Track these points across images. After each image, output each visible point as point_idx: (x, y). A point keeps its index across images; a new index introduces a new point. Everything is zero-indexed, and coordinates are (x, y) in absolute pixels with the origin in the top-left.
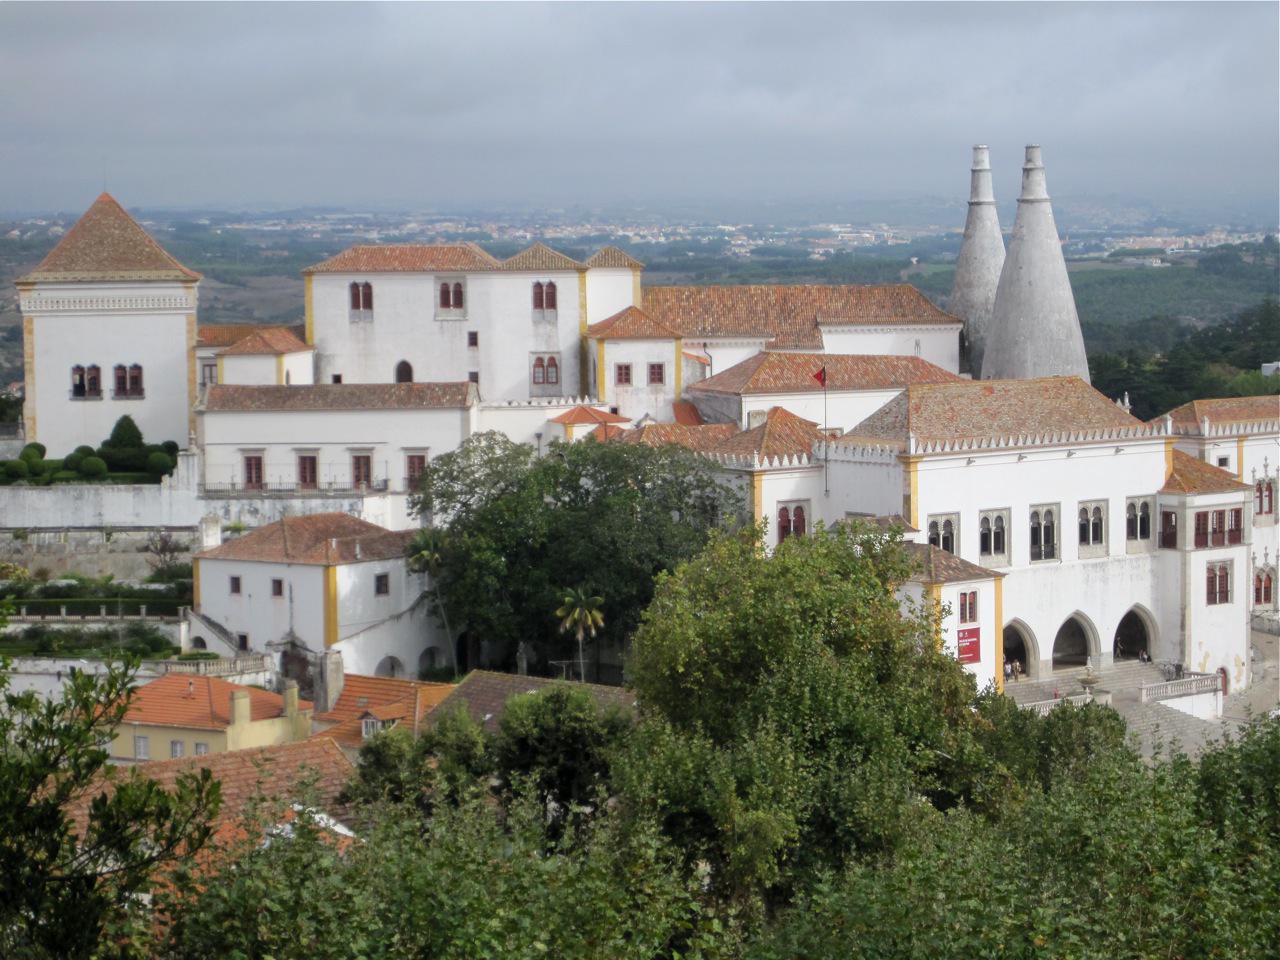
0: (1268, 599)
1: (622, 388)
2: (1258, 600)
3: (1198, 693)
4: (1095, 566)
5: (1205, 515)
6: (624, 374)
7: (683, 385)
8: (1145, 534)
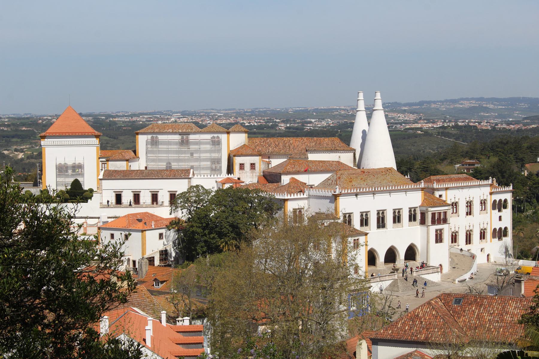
0: (455, 242)
1: (241, 171)
2: (452, 242)
5: (435, 213)
6: (242, 166)
7: (262, 170)
8: (415, 220)
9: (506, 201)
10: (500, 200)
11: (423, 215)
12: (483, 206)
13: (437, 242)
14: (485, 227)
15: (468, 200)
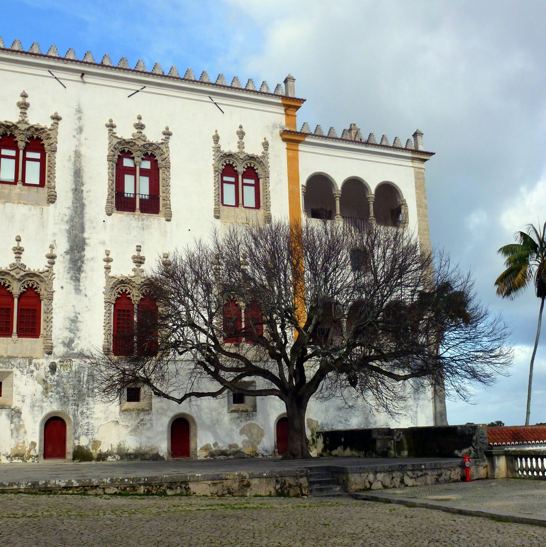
15: (126, 132)
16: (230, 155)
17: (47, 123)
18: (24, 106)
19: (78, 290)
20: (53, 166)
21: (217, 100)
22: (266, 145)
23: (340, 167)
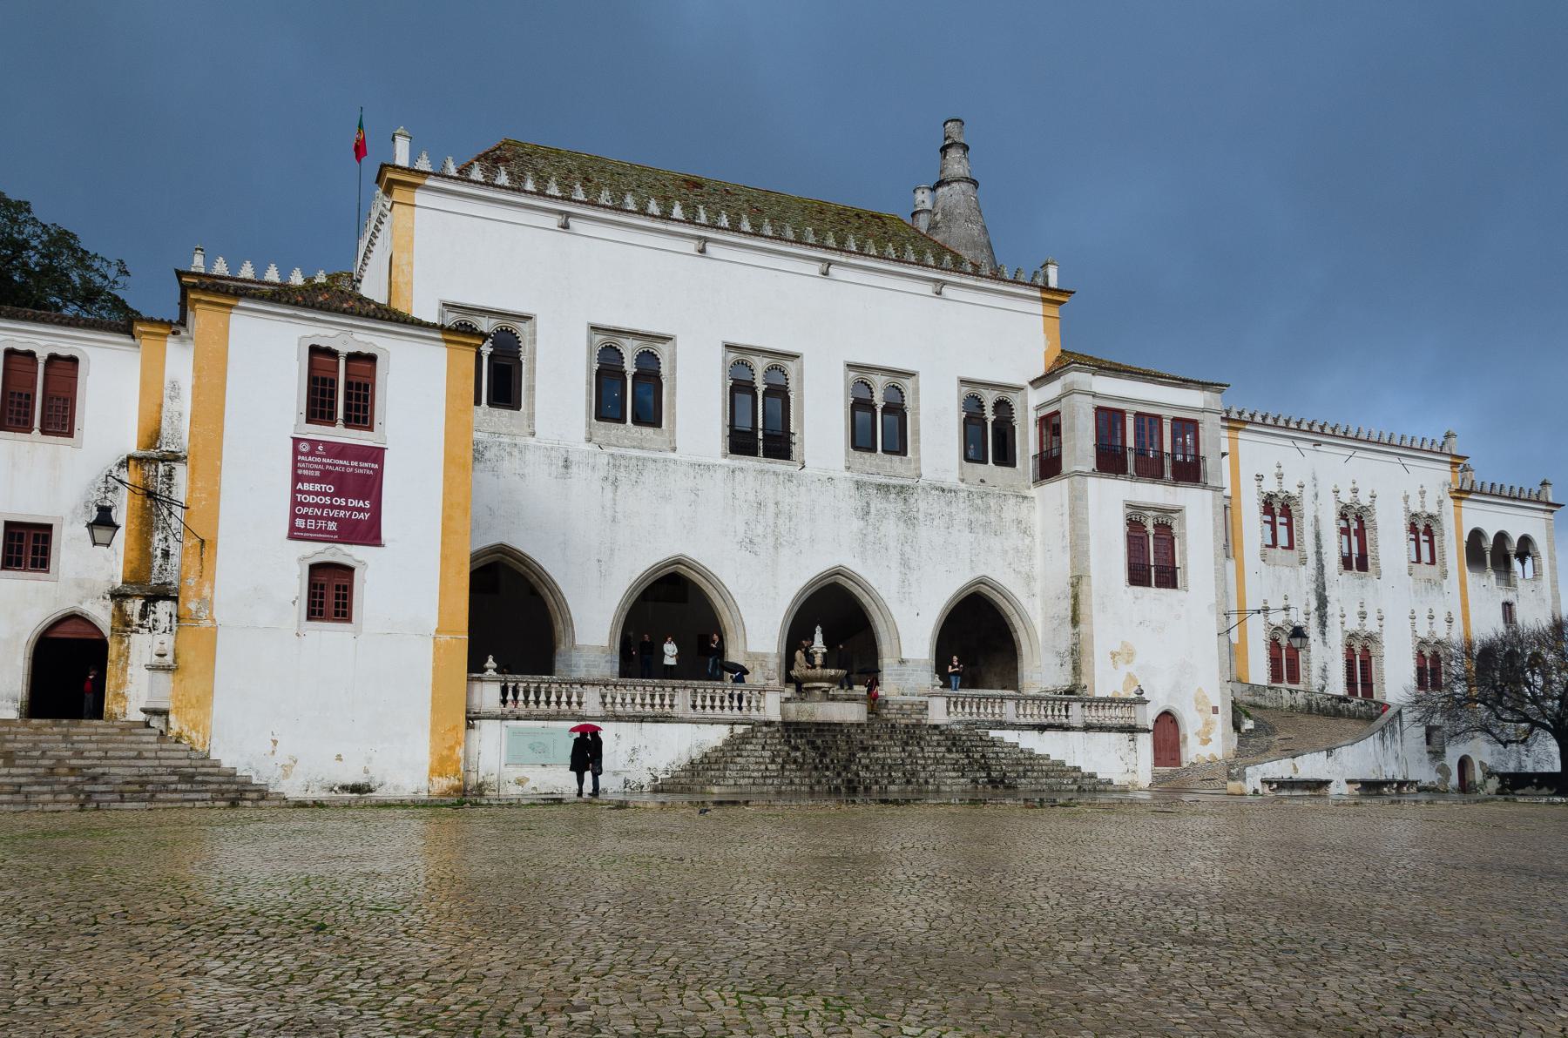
0: (1294, 677)
3: (1088, 728)
4: (883, 488)
8: (1005, 456)
9: (1525, 541)
10: (1501, 537)
11: (1050, 425)
12: (1425, 547)
13: (1138, 576)
14: (1441, 634)
15: (1346, 498)
16: (1415, 515)
17: (1294, 492)
18: (1280, 476)
19: (1325, 643)
20: (1301, 532)
21: (1404, 461)
22: (1440, 502)
23: (1492, 520)
